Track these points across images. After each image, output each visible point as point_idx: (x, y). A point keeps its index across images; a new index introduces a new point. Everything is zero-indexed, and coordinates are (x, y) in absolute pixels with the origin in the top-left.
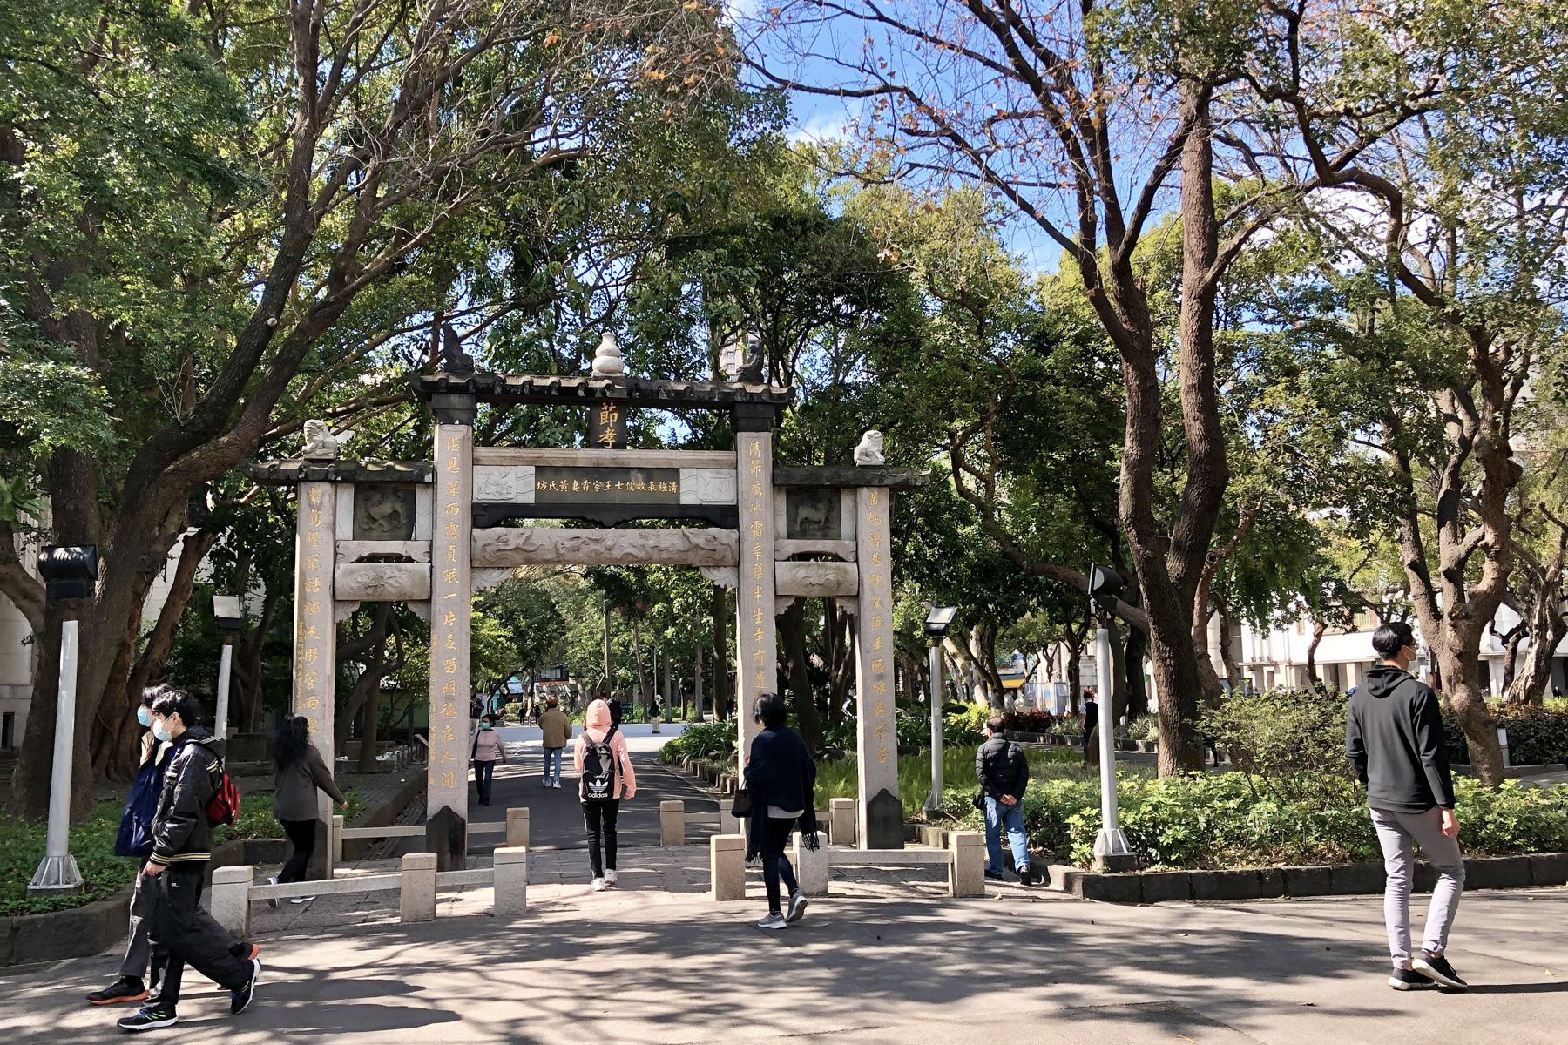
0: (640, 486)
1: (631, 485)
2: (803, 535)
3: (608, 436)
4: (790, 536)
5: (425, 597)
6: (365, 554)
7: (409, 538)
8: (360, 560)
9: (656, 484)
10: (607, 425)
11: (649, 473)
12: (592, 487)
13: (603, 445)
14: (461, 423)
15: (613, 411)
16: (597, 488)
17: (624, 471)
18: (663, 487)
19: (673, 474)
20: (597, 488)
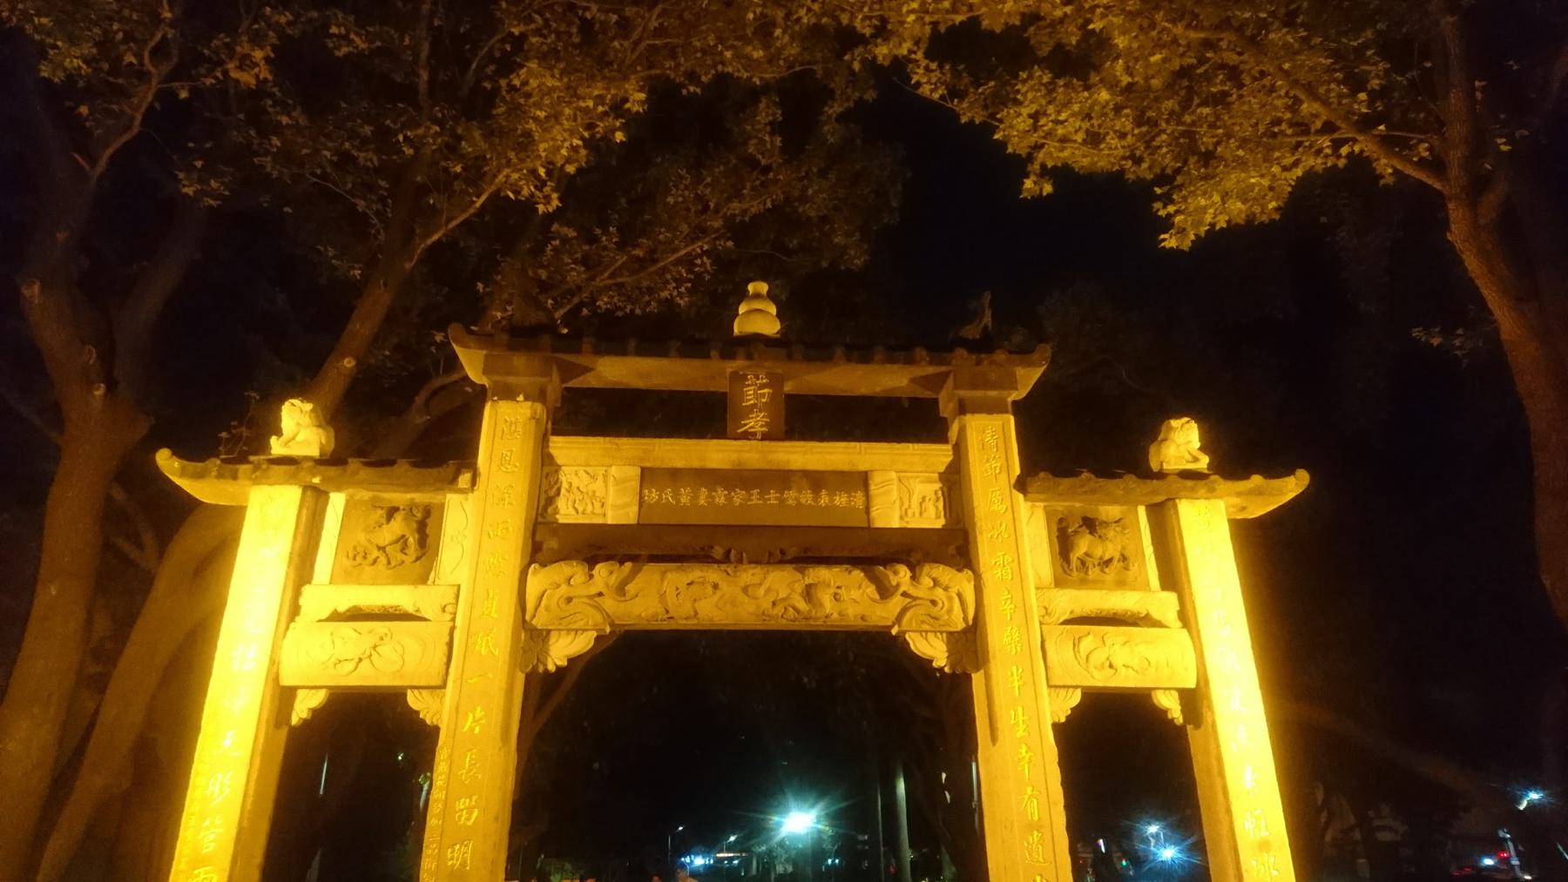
0: (807, 498)
1: (791, 496)
2: (1084, 583)
3: (756, 422)
4: (1059, 583)
5: (438, 682)
6: (342, 608)
7: (423, 579)
8: (336, 617)
9: (831, 494)
10: (754, 405)
11: (817, 480)
12: (729, 499)
13: (747, 436)
14: (526, 399)
15: (763, 386)
16: (737, 501)
17: (782, 478)
18: (841, 500)
19: (861, 480)
20: (737, 501)
